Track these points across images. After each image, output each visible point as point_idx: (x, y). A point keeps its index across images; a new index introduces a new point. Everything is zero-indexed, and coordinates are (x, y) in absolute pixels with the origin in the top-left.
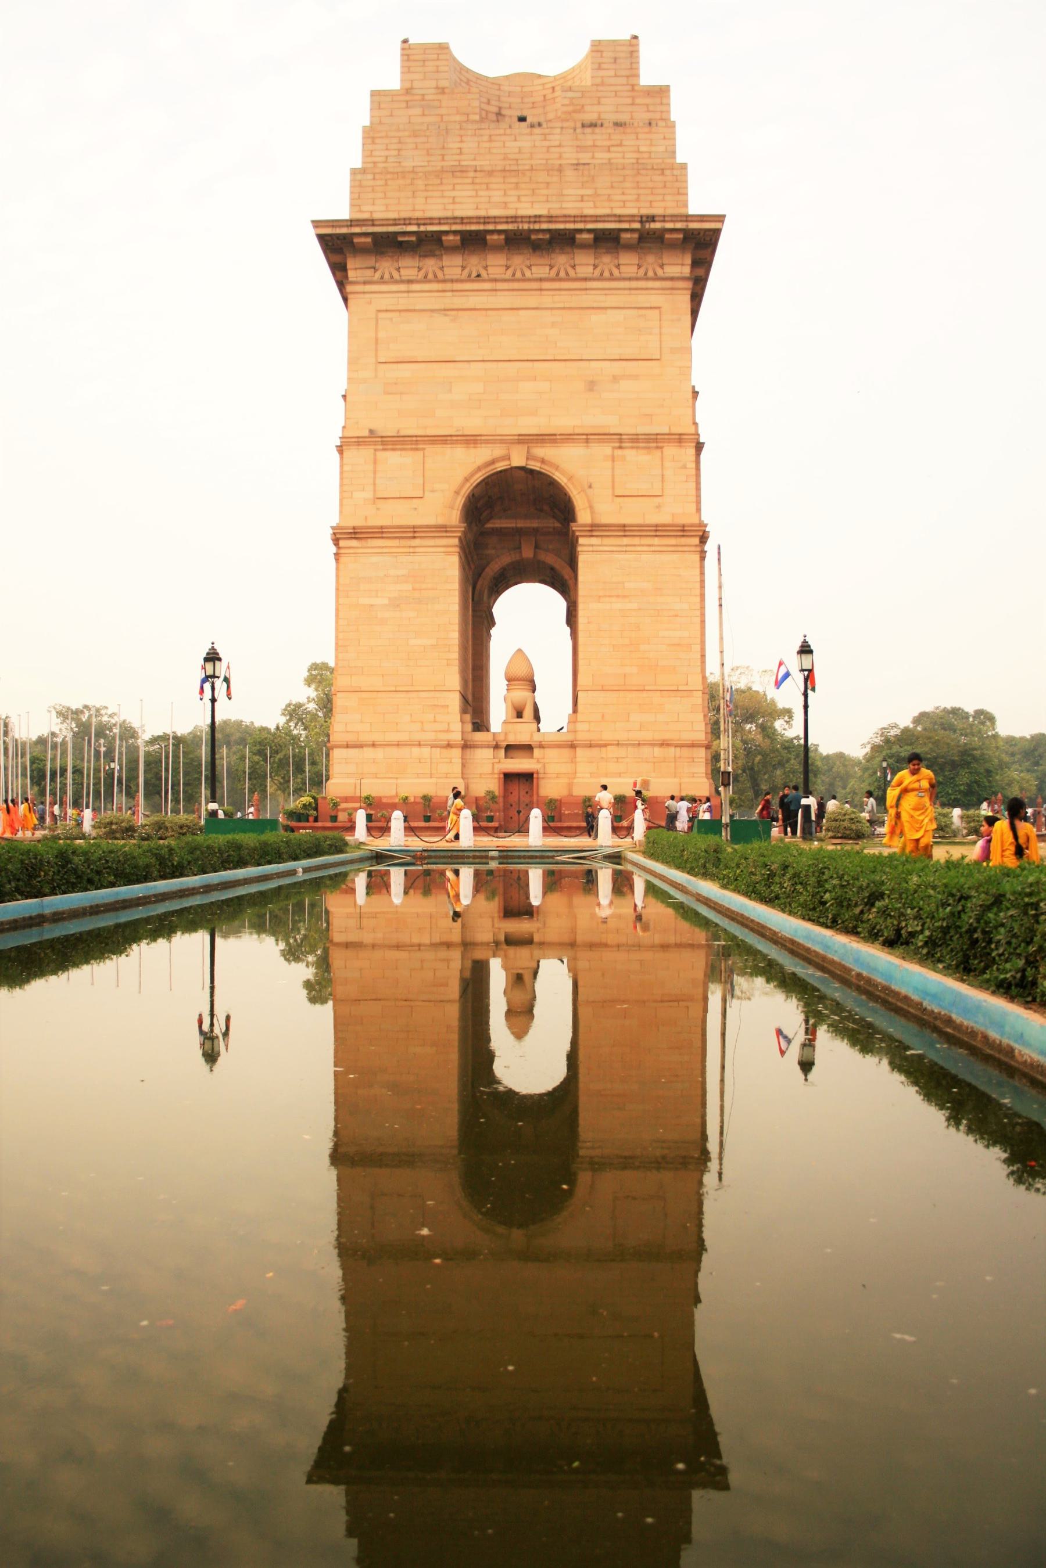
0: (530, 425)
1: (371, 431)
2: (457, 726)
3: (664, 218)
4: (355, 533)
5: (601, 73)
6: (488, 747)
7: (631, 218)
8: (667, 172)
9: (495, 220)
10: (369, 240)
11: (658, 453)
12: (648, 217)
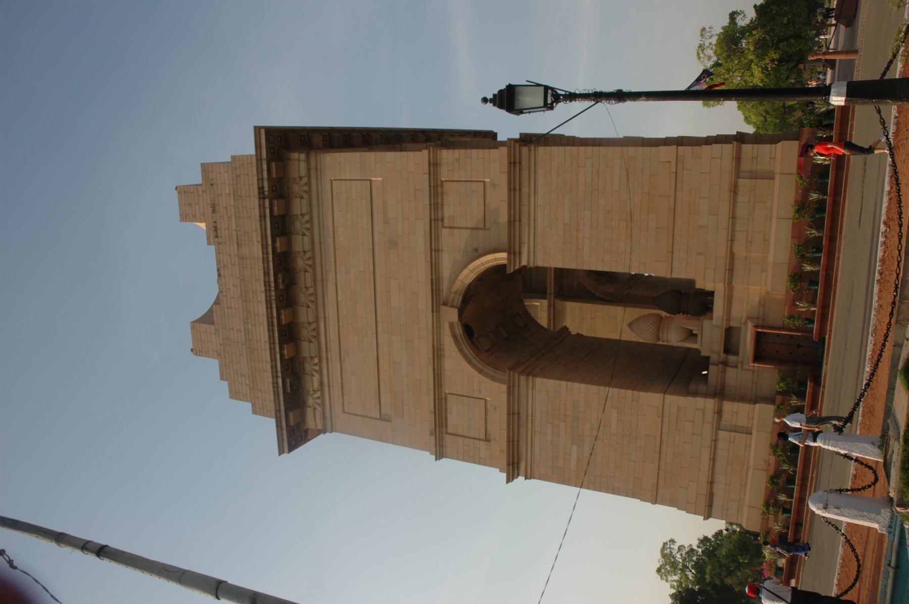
0: (424, 301)
1: (431, 434)
2: (700, 401)
3: (260, 180)
4: (513, 463)
6: (724, 372)
7: (262, 206)
8: (238, 172)
10: (291, 414)
11: (446, 185)
12: (259, 193)
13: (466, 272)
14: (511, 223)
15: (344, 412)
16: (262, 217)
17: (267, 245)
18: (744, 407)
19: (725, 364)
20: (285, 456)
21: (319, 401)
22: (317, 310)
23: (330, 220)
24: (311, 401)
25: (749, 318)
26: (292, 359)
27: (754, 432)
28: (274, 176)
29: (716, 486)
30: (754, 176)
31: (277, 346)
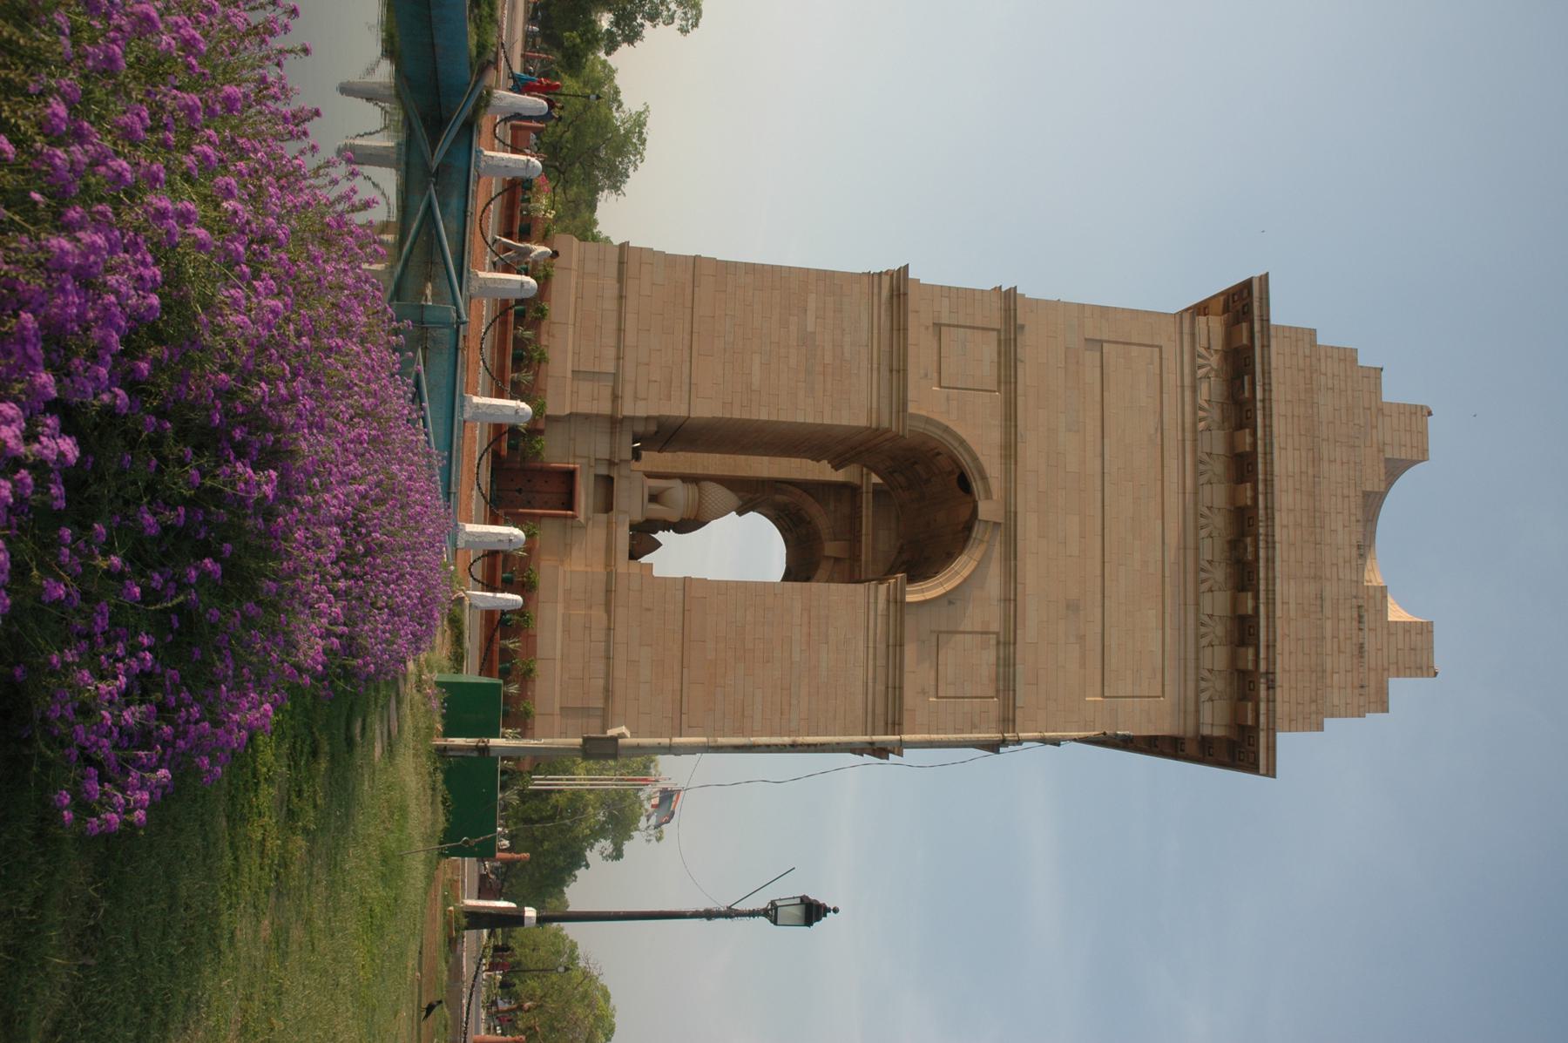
0: (1028, 525)
1: (1022, 327)
2: (641, 411)
3: (1271, 701)
7: (1271, 661)
8: (1313, 707)
9: (1270, 493)
10: (1245, 341)
13: (966, 573)
14: (900, 645)
15: (1160, 348)
16: (1271, 646)
17: (1267, 604)
18: (584, 407)
19: (611, 463)
20: (1256, 273)
21: (1200, 361)
22: (1196, 504)
23: (1168, 640)
24: (1214, 360)
25: (583, 527)
27: (569, 374)
29: (615, 292)
31: (1260, 449)
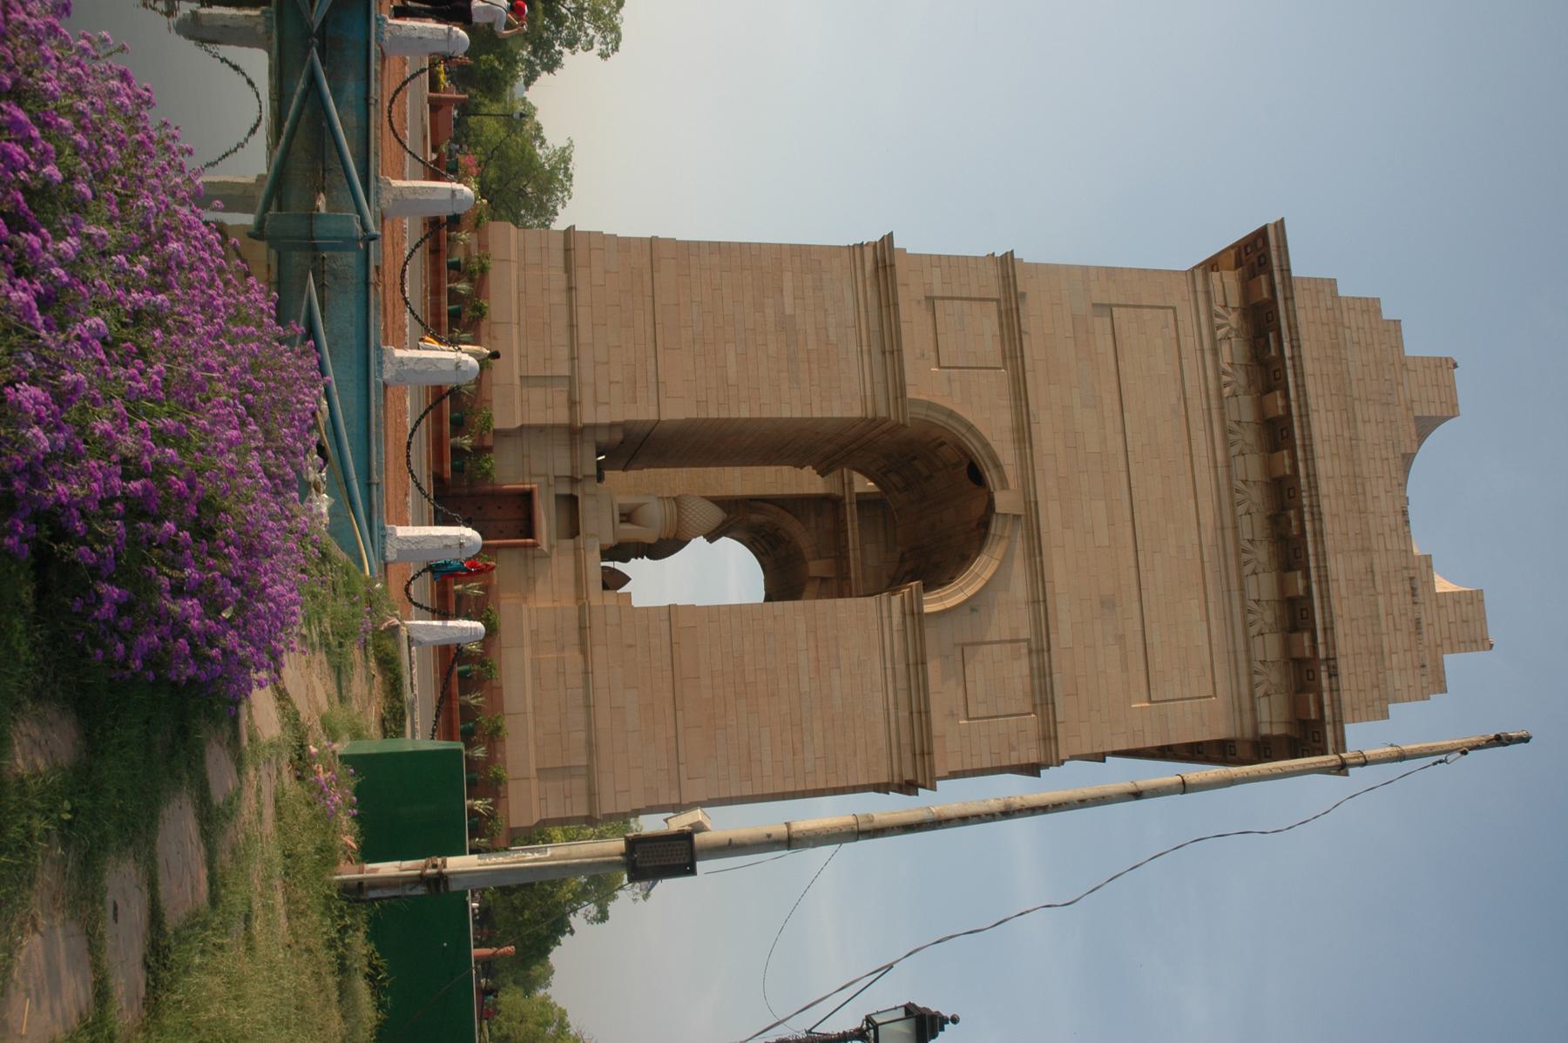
0: (1051, 517)
2: (604, 417)
3: (1335, 690)
4: (885, 267)
5: (1450, 603)
7: (1331, 645)
8: (1376, 693)
9: (1310, 458)
10: (1266, 295)
12: (1335, 667)
13: (987, 574)
14: (922, 662)
15: (1174, 309)
16: (1329, 629)
17: (1319, 582)
18: (537, 418)
19: (573, 480)
20: (1271, 220)
21: (1218, 321)
22: (1230, 478)
23: (1214, 631)
24: (1233, 319)
25: (547, 556)
26: (1268, 389)
27: (517, 381)
28: (1311, 697)
29: (563, 284)
30: (566, 771)
31: (1294, 411)
